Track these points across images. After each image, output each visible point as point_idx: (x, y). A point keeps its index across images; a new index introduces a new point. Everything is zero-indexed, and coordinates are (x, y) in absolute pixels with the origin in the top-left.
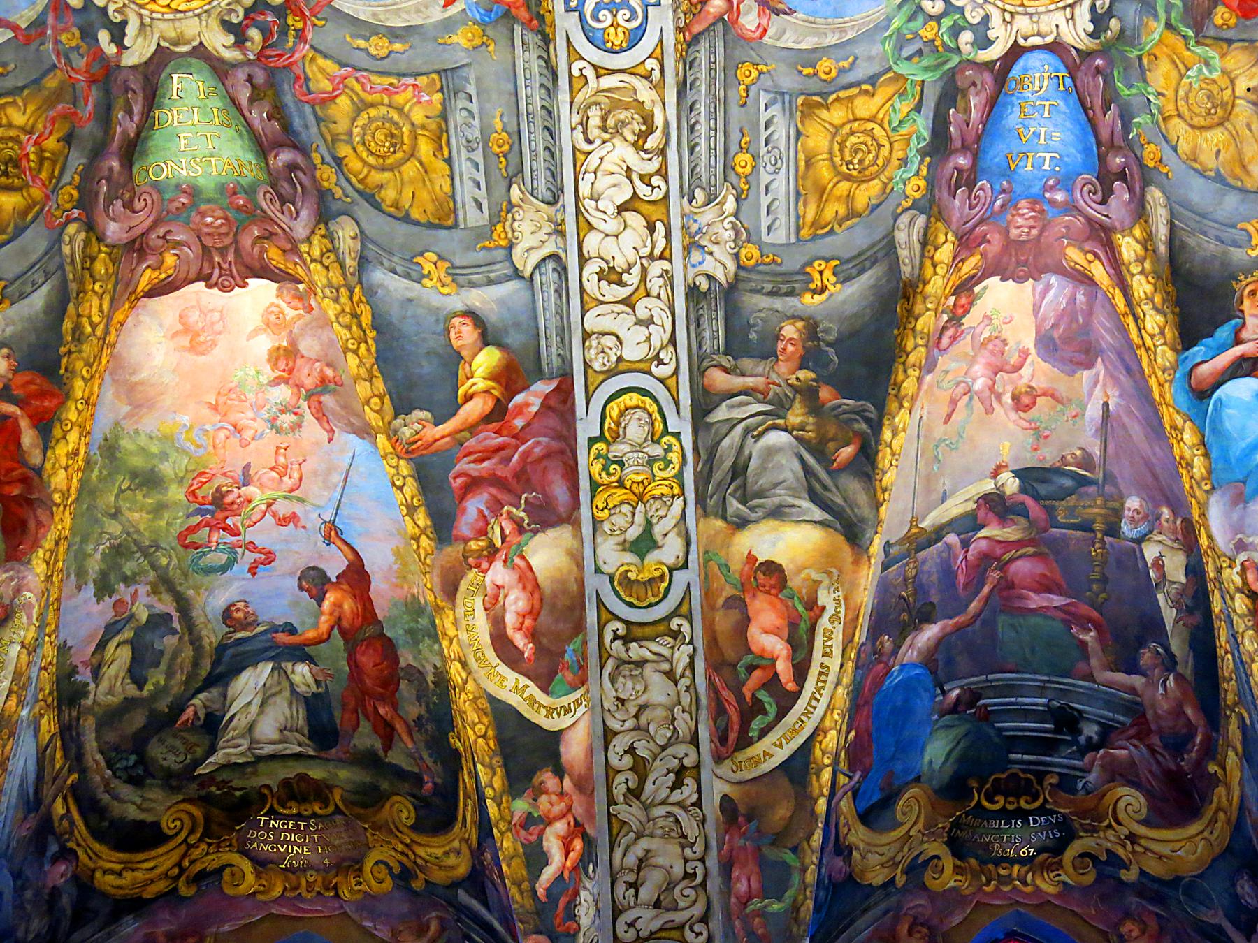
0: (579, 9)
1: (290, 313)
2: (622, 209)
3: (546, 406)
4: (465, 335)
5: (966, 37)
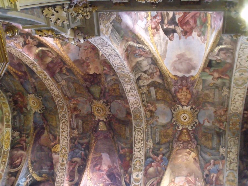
0: (63, 104)
1: (88, 71)
2: (53, 90)
3: (56, 71)
4: (67, 74)
5: (36, 95)
